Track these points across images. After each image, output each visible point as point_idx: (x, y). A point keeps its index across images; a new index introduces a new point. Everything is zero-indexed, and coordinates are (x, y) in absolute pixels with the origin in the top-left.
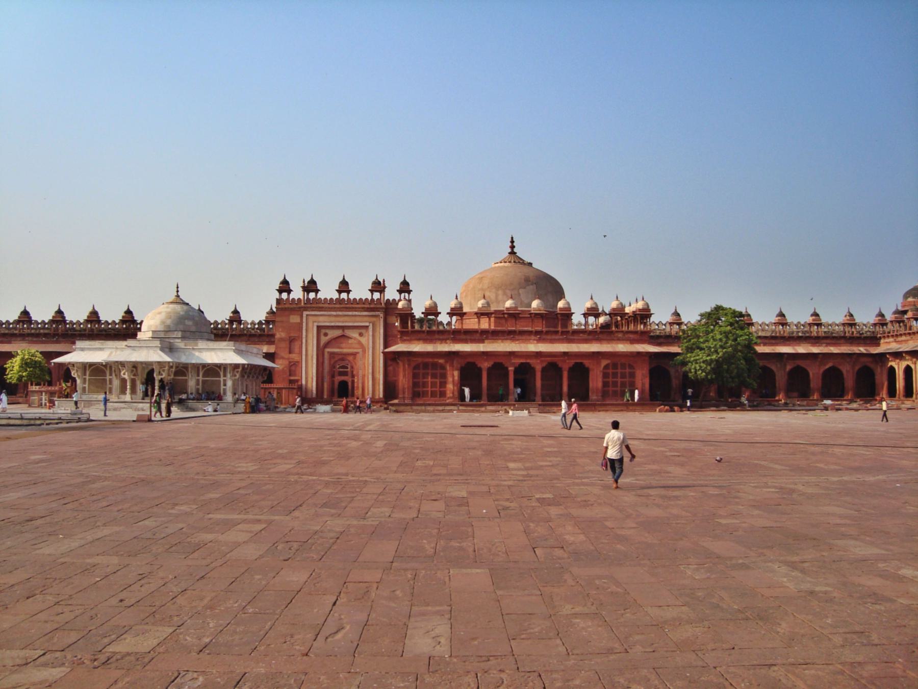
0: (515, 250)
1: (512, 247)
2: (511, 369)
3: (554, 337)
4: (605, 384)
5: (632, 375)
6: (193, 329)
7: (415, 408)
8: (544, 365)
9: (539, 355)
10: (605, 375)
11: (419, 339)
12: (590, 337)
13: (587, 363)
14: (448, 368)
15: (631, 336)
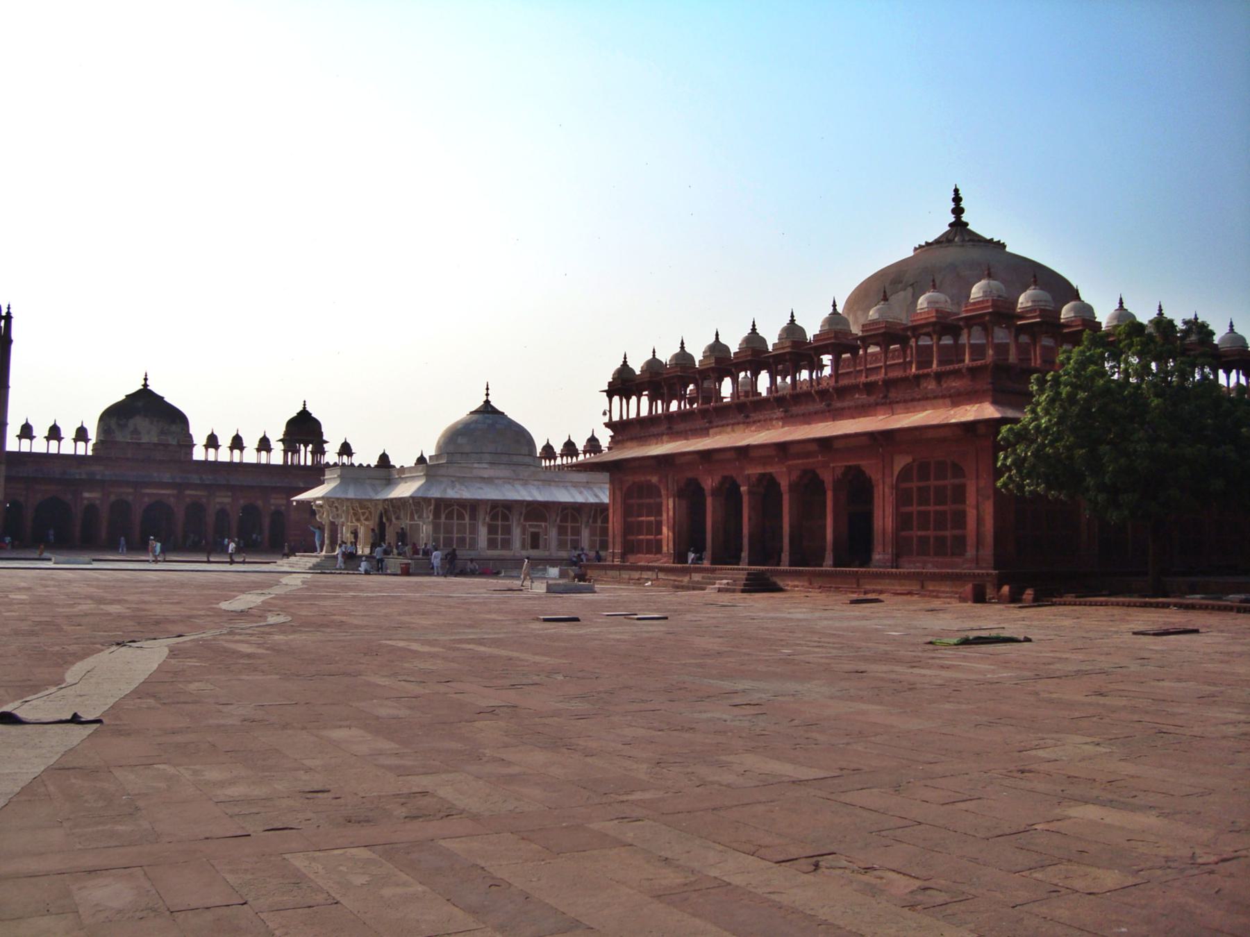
0: (965, 218)
1: (958, 211)
2: (743, 489)
3: (811, 408)
4: (903, 521)
5: (959, 494)
6: (467, 449)
7: (625, 575)
8: (795, 475)
9: (782, 448)
10: (903, 498)
11: (632, 439)
12: (872, 399)
13: (870, 466)
14: (663, 492)
15: (956, 384)
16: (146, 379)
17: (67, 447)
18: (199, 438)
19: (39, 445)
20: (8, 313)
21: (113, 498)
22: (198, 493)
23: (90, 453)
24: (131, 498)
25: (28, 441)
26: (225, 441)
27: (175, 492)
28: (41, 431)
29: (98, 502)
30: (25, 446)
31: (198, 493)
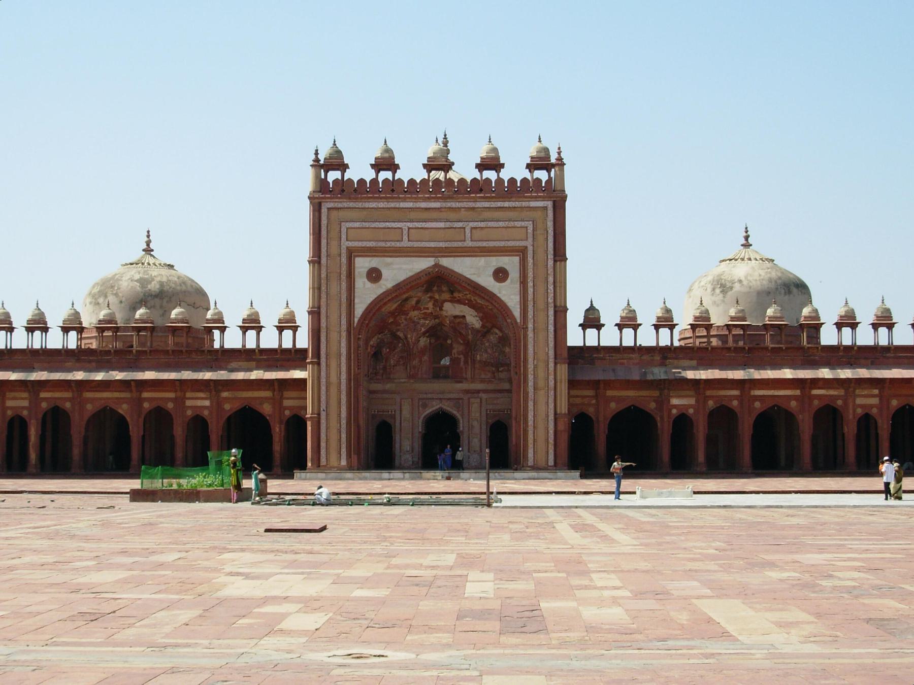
16: (747, 238)
17: (647, 338)
18: (829, 317)
19: (609, 337)
20: (560, 159)
21: (711, 403)
22: (832, 392)
23: (676, 343)
24: (735, 403)
25: (595, 331)
26: (865, 317)
27: (798, 392)
28: (610, 317)
29: (691, 411)
30: (592, 338)
31: (832, 392)
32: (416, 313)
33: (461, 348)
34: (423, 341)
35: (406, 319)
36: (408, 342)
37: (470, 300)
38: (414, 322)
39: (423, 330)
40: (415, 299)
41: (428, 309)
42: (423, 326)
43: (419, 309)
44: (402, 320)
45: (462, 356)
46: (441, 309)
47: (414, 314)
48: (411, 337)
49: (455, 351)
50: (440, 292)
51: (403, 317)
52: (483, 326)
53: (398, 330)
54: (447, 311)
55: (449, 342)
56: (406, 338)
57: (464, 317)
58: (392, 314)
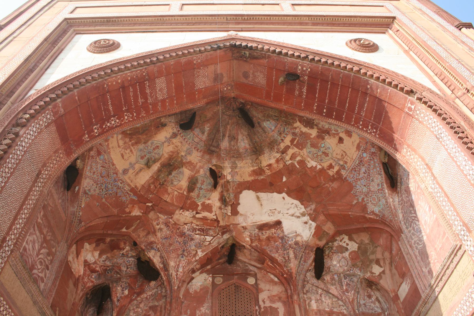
32: (187, 215)
33: (277, 290)
34: (201, 280)
35: (167, 224)
36: (169, 276)
37: (290, 170)
38: (182, 235)
39: (200, 254)
40: (187, 172)
41: (208, 208)
42: (199, 245)
43: (193, 207)
44: (158, 220)
45: (280, 306)
46: (235, 212)
47: (184, 217)
48: (177, 267)
49: (262, 296)
50: (236, 155)
51: (163, 217)
52: (319, 233)
53: (151, 245)
54: (245, 216)
55: (251, 281)
56: (166, 268)
57: (278, 223)
58: (140, 197)
